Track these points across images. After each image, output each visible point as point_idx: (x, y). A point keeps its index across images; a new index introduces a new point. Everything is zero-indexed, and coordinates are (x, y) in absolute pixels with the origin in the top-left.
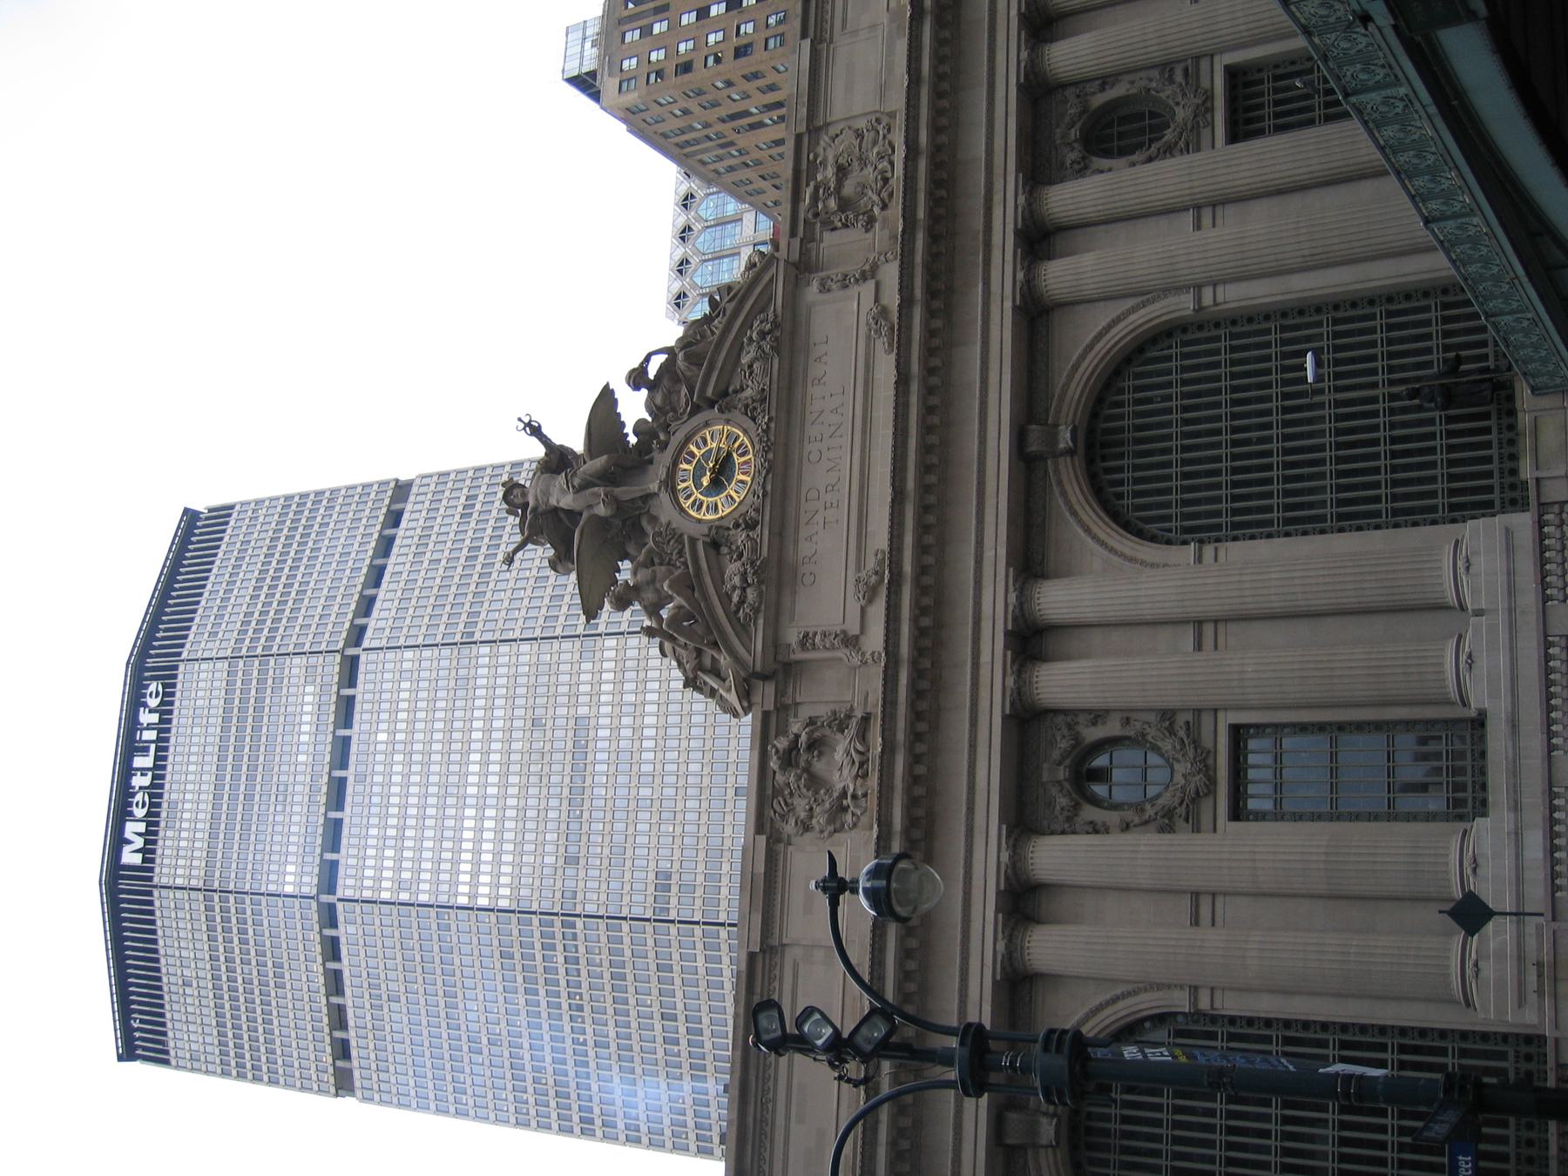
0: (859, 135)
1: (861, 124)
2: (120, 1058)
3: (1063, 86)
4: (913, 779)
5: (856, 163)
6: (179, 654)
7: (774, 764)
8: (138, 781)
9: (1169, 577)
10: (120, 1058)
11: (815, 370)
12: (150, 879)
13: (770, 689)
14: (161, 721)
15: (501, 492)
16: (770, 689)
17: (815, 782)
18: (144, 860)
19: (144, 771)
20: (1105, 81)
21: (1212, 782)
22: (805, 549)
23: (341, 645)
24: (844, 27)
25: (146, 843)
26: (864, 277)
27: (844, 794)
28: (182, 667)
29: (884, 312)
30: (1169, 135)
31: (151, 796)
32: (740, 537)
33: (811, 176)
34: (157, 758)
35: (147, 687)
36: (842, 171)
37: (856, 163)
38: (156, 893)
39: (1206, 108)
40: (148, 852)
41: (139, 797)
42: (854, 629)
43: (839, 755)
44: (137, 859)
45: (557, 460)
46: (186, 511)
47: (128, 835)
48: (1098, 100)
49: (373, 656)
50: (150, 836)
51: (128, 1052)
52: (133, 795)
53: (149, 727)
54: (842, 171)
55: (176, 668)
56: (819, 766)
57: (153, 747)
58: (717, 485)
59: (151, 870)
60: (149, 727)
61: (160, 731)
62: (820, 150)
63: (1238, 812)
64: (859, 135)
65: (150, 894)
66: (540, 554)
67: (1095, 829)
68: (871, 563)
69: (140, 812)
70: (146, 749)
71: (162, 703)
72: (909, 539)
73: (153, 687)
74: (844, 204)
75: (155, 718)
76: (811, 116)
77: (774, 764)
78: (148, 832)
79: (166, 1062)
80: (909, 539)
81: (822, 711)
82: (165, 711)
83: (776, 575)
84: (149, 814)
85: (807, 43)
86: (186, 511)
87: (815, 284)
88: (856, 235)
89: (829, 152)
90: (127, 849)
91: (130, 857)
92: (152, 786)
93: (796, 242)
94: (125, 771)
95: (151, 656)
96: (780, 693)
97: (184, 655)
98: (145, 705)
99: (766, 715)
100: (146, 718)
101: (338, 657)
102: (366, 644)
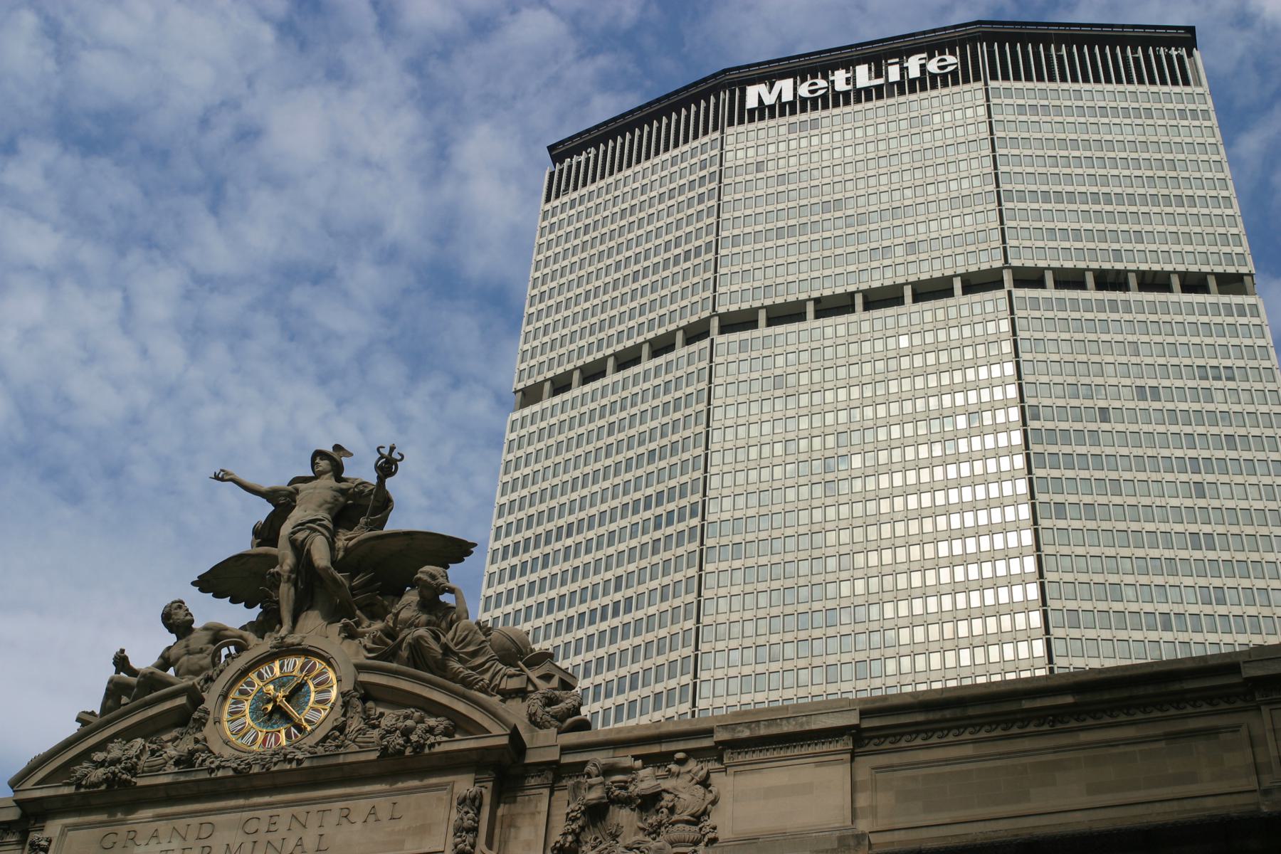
0: (696, 819)
2: (551, 148)
5: (653, 819)
10: (551, 148)
12: (731, 124)
18: (752, 111)
23: (1015, 263)
24: (878, 769)
25: (772, 107)
28: (980, 84)
31: (824, 97)
33: (648, 760)
34: (868, 90)
35: (953, 53)
37: (653, 819)
38: (717, 135)
40: (763, 111)
41: (822, 83)
44: (751, 102)
45: (361, 505)
46: (1191, 30)
47: (779, 84)
49: (1003, 305)
50: (781, 109)
51: (559, 152)
52: (825, 77)
53: (903, 70)
54: (649, 802)
55: (977, 79)
57: (881, 81)
59: (741, 122)
60: (903, 70)
61: (900, 84)
62: (692, 765)
65: (715, 129)
66: (264, 510)
69: (804, 90)
70: (878, 75)
71: (933, 76)
73: (951, 59)
75: (914, 72)
78: (783, 106)
79: (548, 200)
82: (926, 82)
84: (804, 100)
85: (852, 719)
86: (1191, 30)
90: (762, 88)
92: (836, 95)
93: (553, 755)
94: (847, 58)
95: (990, 47)
97: (992, 84)
98: (931, 56)
100: (914, 65)
101: (998, 264)
102: (1018, 293)
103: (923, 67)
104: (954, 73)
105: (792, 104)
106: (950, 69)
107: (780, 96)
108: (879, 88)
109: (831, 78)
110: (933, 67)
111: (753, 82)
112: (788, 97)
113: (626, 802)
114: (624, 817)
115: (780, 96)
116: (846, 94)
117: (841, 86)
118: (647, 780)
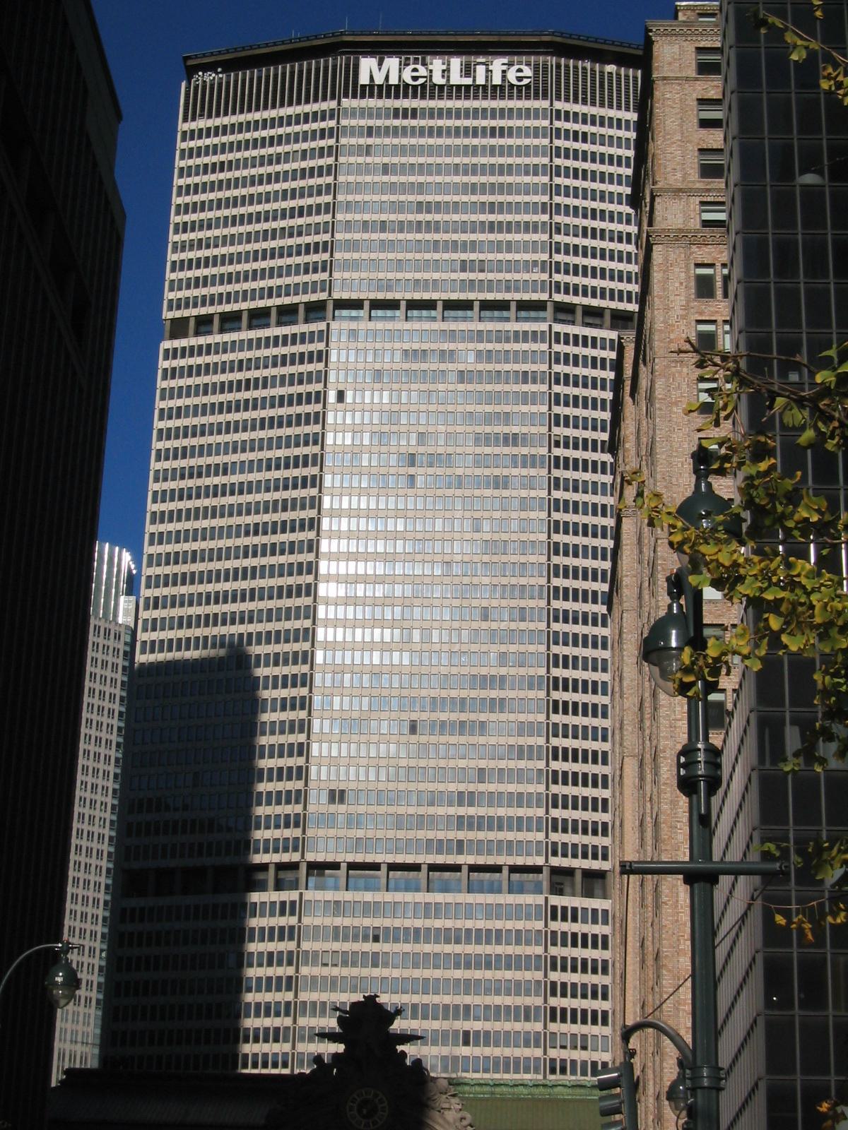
6: (558, 98)
8: (437, 64)
12: (346, 96)
14: (494, 87)
18: (363, 86)
19: (446, 72)
25: (380, 87)
31: (423, 86)
34: (459, 87)
35: (528, 64)
38: (333, 104)
40: (371, 90)
41: (422, 71)
44: (364, 79)
52: (424, 64)
55: (545, 97)
57: (468, 81)
65: (333, 98)
69: (407, 76)
70: (467, 74)
75: (497, 80)
78: (389, 87)
91: (368, 68)
98: (510, 64)
100: (498, 64)
103: (504, 72)
104: (528, 86)
105: (397, 87)
106: (526, 81)
107: (387, 78)
108: (467, 87)
109: (430, 67)
110: (512, 76)
111: (366, 54)
112: (394, 80)
115: (387, 78)
116: (441, 87)
117: (438, 79)
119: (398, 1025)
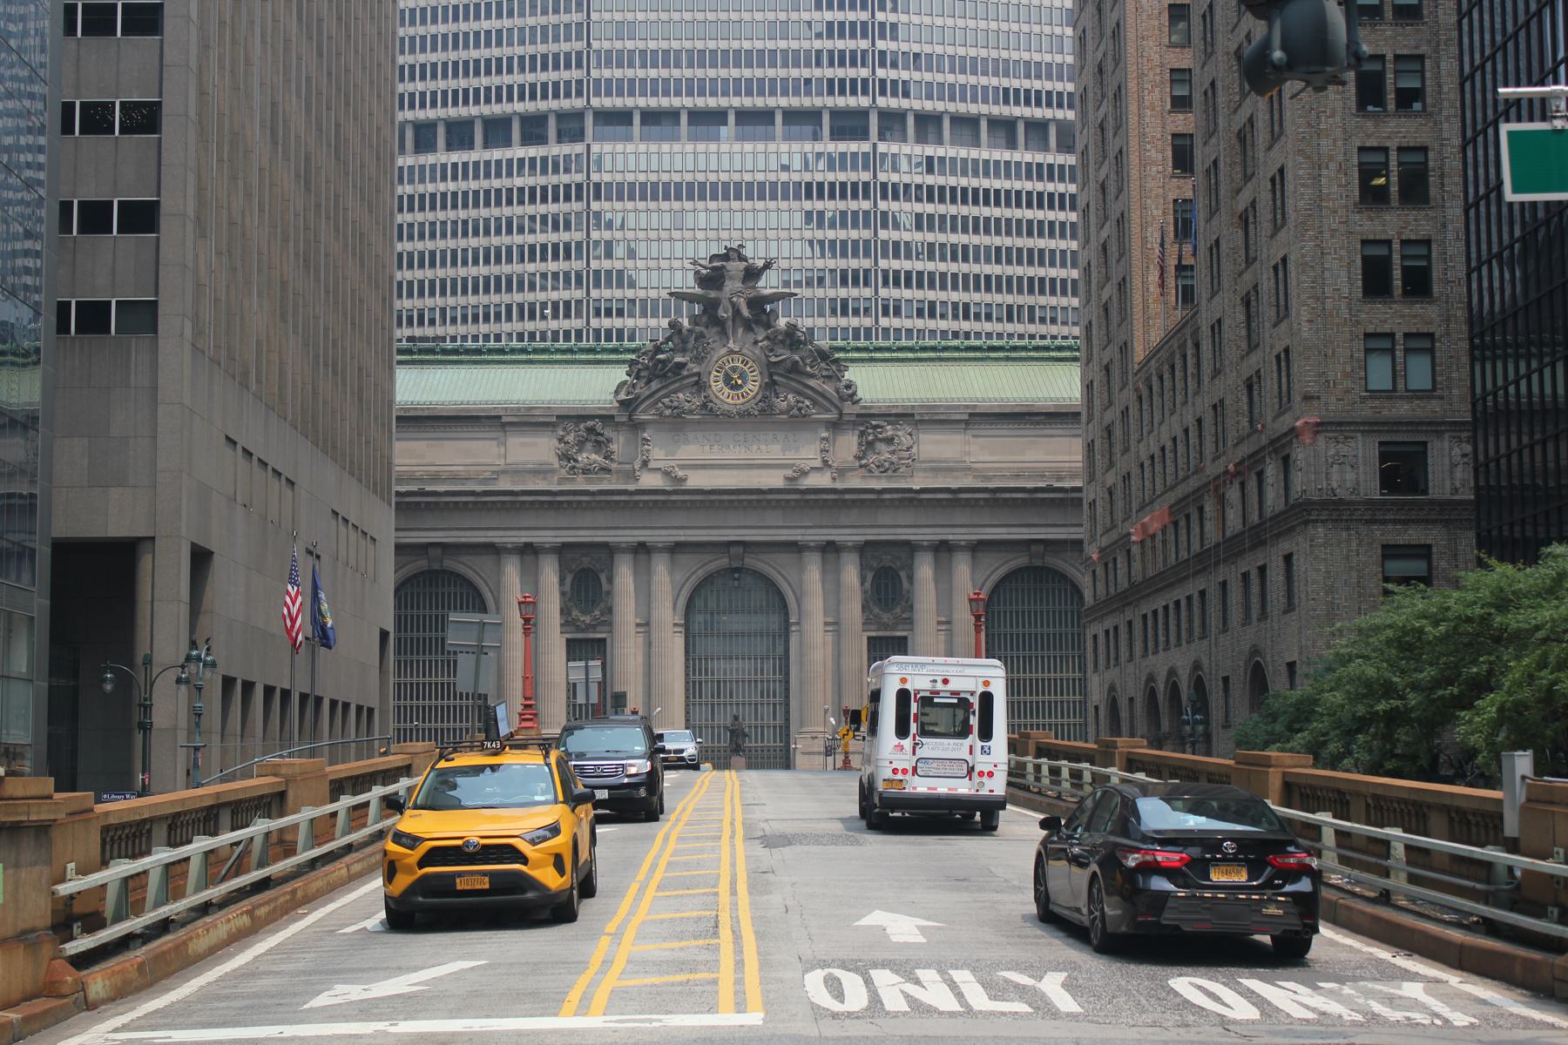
0: (908, 449)
1: (914, 450)
3: (912, 558)
4: (580, 502)
7: (590, 423)
9: (667, 614)
11: (781, 436)
13: (624, 419)
15: (735, 245)
16: (624, 419)
17: (581, 444)
20: (911, 578)
21: (583, 631)
22: (691, 435)
26: (825, 462)
27: (576, 461)
29: (804, 473)
30: (876, 610)
32: (697, 402)
36: (889, 441)
39: (886, 627)
42: (652, 465)
43: (594, 456)
48: (903, 574)
54: (889, 441)
56: (589, 446)
58: (727, 379)
63: (570, 643)
64: (908, 449)
67: (562, 581)
68: (680, 474)
72: (687, 497)
74: (870, 444)
76: (921, 421)
77: (590, 423)
80: (687, 497)
81: (613, 447)
83: (677, 422)
87: (825, 435)
88: (854, 449)
89: (903, 435)
96: (623, 424)
99: (612, 417)
113: (881, 440)
114: (881, 447)
118: (889, 431)
119: (769, 284)
